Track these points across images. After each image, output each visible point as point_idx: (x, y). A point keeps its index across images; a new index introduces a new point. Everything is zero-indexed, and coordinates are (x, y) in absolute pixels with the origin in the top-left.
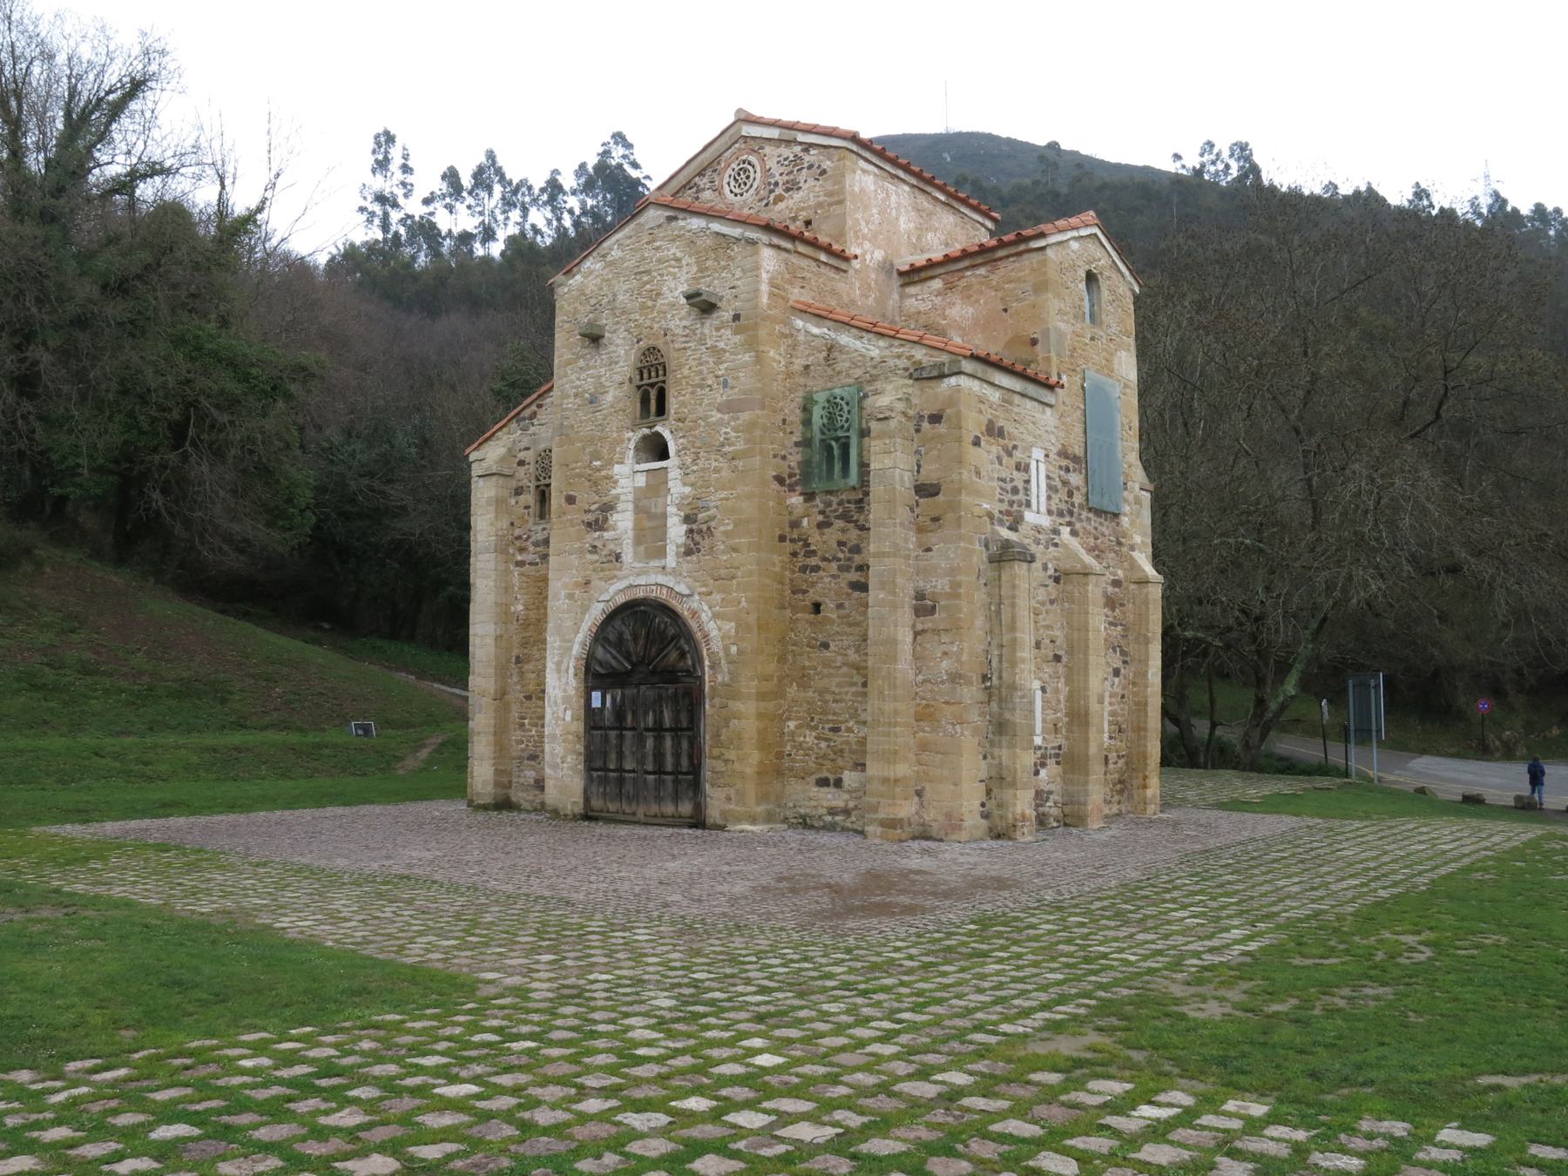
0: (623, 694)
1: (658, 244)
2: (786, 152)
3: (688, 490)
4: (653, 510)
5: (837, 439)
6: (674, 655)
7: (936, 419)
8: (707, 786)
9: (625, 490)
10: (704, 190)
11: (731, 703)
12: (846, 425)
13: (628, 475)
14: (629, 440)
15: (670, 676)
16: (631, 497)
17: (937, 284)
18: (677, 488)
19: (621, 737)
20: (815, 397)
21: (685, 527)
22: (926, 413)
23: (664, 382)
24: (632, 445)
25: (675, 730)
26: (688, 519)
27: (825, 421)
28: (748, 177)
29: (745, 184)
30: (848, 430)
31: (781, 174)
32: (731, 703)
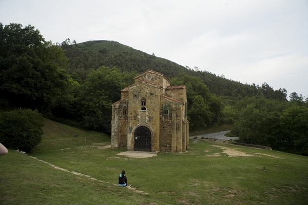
13: (140, 111)
15: (147, 134)
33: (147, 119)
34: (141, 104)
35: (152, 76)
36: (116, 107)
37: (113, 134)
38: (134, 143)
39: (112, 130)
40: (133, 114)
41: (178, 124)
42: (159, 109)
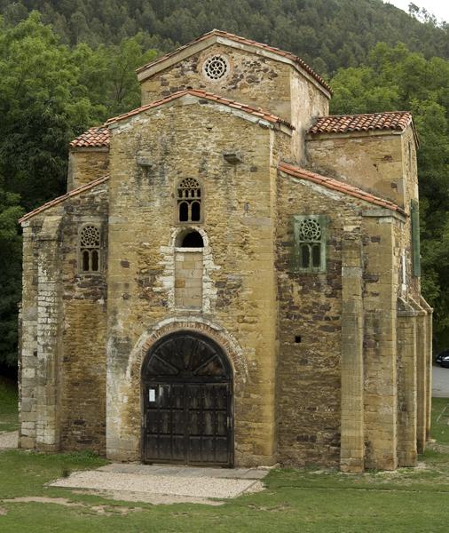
0: (173, 389)
1: (194, 115)
2: (248, 59)
3: (219, 267)
5: (311, 244)
6: (211, 366)
7: (376, 239)
8: (236, 444)
10: (189, 70)
11: (252, 395)
12: (318, 237)
13: (169, 252)
14: (172, 232)
15: (210, 377)
16: (172, 268)
17: (330, 144)
19: (171, 416)
20: (296, 217)
21: (216, 290)
22: (370, 235)
23: (200, 200)
24: (174, 235)
25: (213, 410)
26: (217, 284)
27: (303, 232)
28: (220, 68)
29: (219, 72)
30: (319, 239)
31: (245, 71)
32: (252, 395)
33: (211, 292)
34: (176, 213)
35: (236, 63)
36: (43, 233)
37: (27, 373)
38: (140, 420)
39: (25, 353)
40: (134, 267)
41: (374, 321)
42: (272, 240)
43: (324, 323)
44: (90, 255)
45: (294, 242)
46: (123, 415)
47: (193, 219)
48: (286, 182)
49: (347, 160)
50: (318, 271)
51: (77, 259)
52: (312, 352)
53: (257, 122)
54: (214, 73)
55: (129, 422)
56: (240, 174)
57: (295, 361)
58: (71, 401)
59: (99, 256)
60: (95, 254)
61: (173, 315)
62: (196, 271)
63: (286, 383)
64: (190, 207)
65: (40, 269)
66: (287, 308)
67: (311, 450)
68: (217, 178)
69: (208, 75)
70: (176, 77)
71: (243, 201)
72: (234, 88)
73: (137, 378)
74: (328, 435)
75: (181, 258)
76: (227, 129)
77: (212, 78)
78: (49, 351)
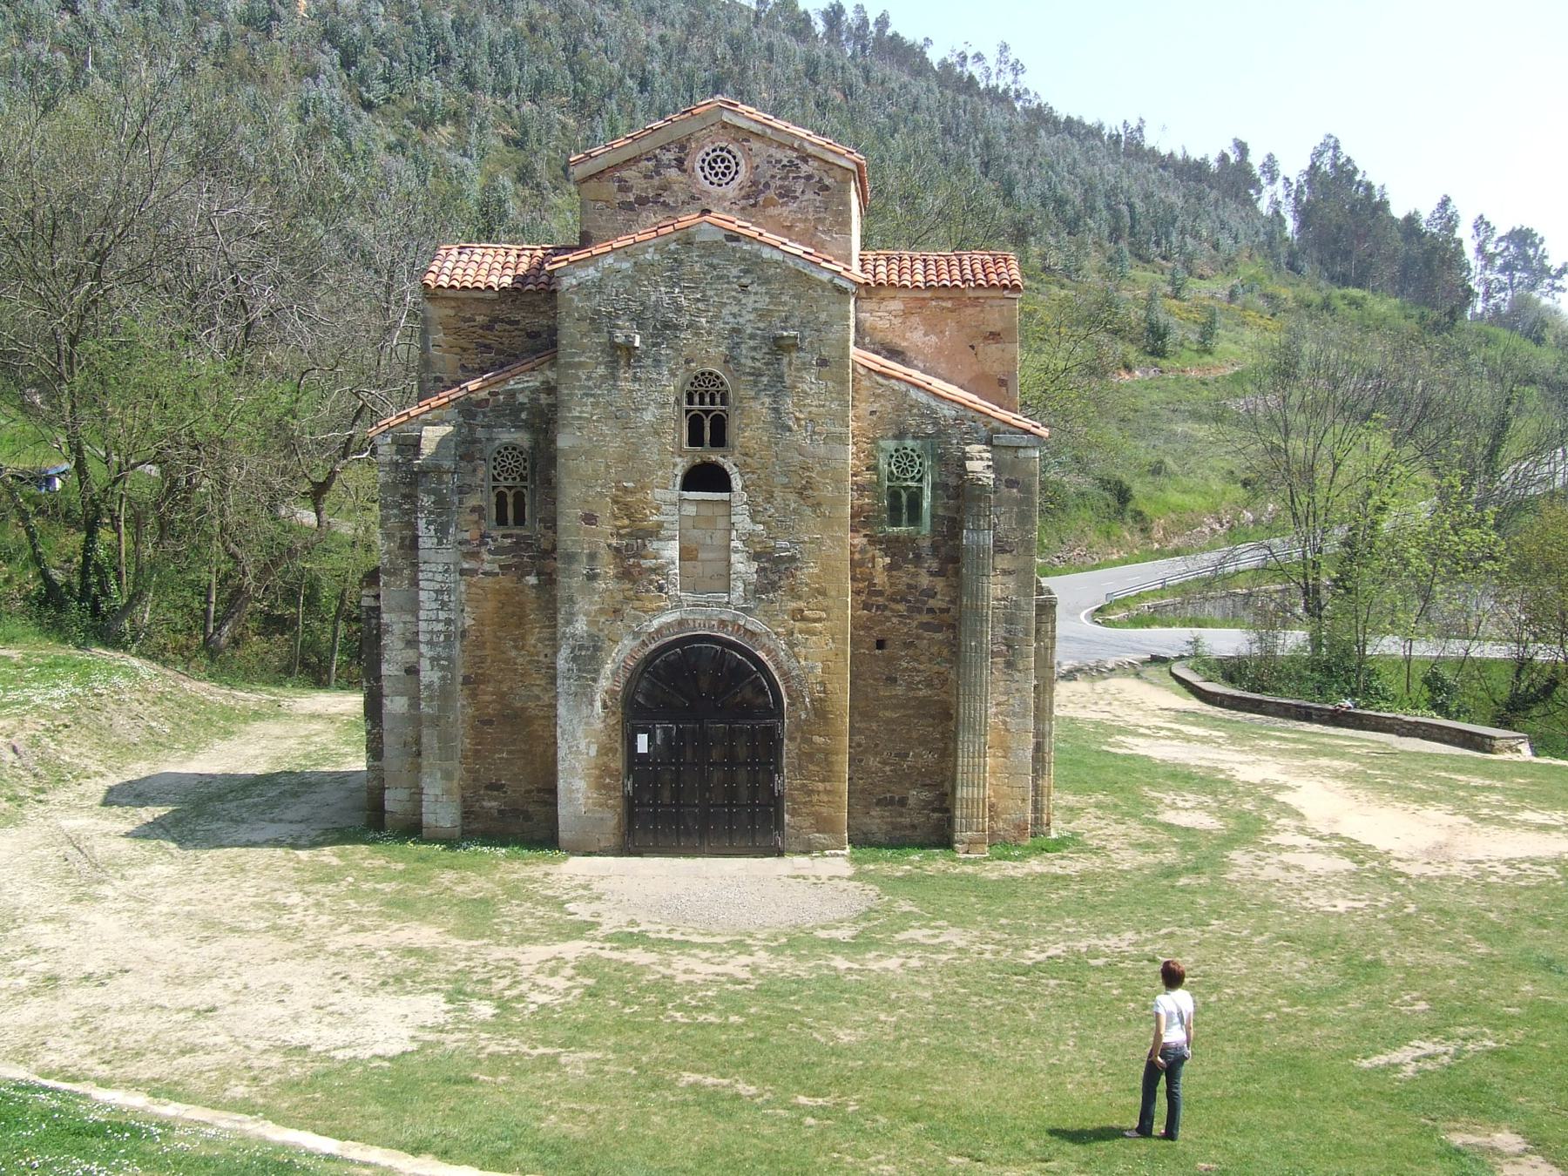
1: (715, 261)
2: (778, 154)
4: (708, 541)
6: (748, 693)
9: (671, 519)
10: (669, 166)
11: (817, 739)
12: (918, 477)
14: (675, 465)
15: (746, 711)
17: (896, 305)
18: (743, 521)
24: (679, 471)
26: (756, 557)
30: (920, 480)
31: (773, 177)
43: (925, 618)
44: (510, 500)
45: (878, 484)
46: (589, 776)
47: (712, 444)
48: (866, 383)
49: (926, 335)
50: (918, 533)
51: (484, 504)
52: (905, 665)
53: (831, 281)
54: (716, 174)
55: (600, 786)
56: (798, 370)
57: (875, 679)
58: (477, 751)
59: (526, 500)
60: (519, 498)
61: (678, 605)
62: (718, 534)
63: (860, 714)
64: (707, 423)
65: (422, 524)
66: (867, 593)
67: (899, 820)
68: (757, 374)
69: (705, 177)
70: (645, 177)
71: (802, 416)
72: (754, 206)
73: (614, 713)
74: (925, 795)
75: (690, 510)
76: (776, 286)
77: (712, 183)
78: (443, 668)
